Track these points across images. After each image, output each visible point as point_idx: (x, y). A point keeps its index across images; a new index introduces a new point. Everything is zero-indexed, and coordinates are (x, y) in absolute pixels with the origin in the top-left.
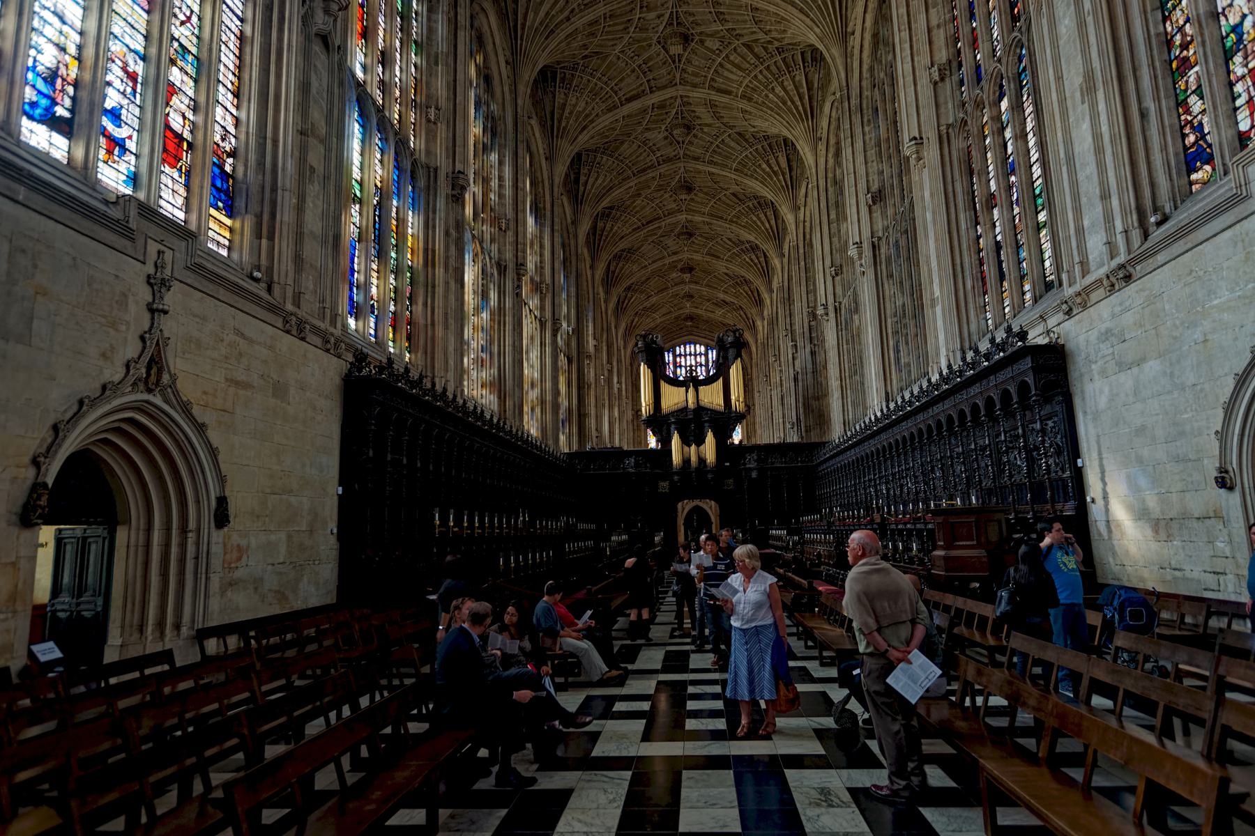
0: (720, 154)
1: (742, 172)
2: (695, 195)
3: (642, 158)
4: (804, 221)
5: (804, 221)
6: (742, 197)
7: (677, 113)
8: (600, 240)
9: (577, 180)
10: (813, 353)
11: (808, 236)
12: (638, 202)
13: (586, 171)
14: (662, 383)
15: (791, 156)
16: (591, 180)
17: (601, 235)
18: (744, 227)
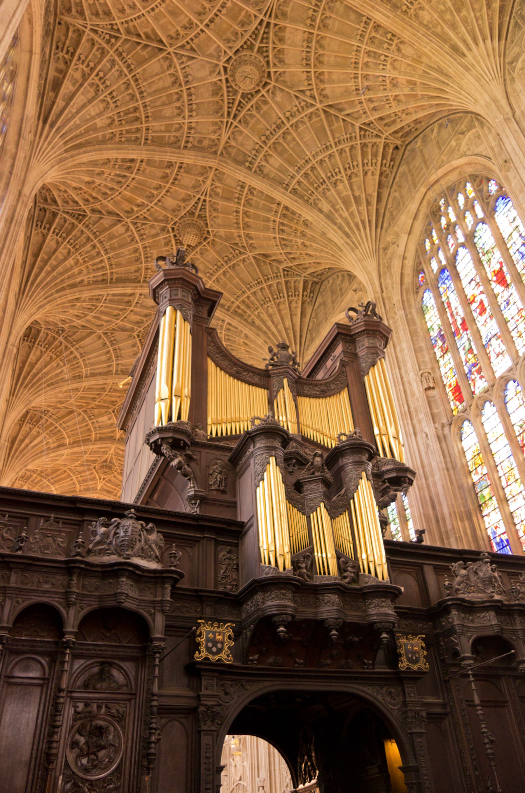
0: (281, 154)
1: (302, 197)
2: (201, 254)
3: (168, 111)
4: (404, 258)
5: (404, 258)
6: (267, 269)
7: (255, 34)
8: (41, 269)
9: (57, 85)
10: (441, 439)
11: (408, 280)
12: (119, 228)
13: (78, 75)
14: (211, 366)
15: (383, 179)
16: (80, 99)
17: (46, 262)
18: (253, 323)
